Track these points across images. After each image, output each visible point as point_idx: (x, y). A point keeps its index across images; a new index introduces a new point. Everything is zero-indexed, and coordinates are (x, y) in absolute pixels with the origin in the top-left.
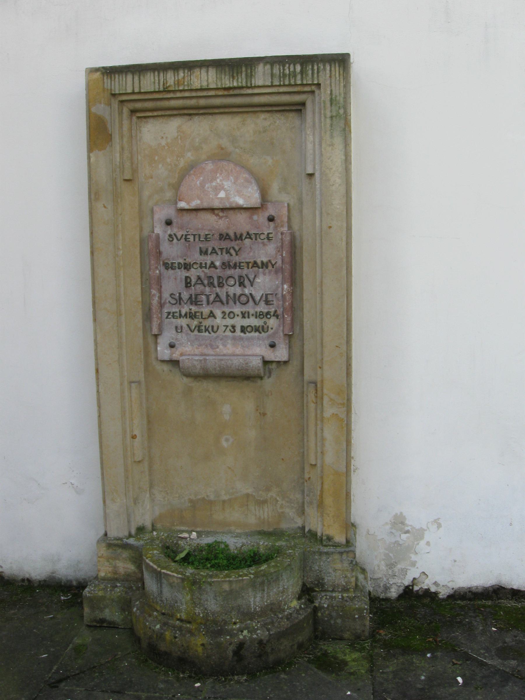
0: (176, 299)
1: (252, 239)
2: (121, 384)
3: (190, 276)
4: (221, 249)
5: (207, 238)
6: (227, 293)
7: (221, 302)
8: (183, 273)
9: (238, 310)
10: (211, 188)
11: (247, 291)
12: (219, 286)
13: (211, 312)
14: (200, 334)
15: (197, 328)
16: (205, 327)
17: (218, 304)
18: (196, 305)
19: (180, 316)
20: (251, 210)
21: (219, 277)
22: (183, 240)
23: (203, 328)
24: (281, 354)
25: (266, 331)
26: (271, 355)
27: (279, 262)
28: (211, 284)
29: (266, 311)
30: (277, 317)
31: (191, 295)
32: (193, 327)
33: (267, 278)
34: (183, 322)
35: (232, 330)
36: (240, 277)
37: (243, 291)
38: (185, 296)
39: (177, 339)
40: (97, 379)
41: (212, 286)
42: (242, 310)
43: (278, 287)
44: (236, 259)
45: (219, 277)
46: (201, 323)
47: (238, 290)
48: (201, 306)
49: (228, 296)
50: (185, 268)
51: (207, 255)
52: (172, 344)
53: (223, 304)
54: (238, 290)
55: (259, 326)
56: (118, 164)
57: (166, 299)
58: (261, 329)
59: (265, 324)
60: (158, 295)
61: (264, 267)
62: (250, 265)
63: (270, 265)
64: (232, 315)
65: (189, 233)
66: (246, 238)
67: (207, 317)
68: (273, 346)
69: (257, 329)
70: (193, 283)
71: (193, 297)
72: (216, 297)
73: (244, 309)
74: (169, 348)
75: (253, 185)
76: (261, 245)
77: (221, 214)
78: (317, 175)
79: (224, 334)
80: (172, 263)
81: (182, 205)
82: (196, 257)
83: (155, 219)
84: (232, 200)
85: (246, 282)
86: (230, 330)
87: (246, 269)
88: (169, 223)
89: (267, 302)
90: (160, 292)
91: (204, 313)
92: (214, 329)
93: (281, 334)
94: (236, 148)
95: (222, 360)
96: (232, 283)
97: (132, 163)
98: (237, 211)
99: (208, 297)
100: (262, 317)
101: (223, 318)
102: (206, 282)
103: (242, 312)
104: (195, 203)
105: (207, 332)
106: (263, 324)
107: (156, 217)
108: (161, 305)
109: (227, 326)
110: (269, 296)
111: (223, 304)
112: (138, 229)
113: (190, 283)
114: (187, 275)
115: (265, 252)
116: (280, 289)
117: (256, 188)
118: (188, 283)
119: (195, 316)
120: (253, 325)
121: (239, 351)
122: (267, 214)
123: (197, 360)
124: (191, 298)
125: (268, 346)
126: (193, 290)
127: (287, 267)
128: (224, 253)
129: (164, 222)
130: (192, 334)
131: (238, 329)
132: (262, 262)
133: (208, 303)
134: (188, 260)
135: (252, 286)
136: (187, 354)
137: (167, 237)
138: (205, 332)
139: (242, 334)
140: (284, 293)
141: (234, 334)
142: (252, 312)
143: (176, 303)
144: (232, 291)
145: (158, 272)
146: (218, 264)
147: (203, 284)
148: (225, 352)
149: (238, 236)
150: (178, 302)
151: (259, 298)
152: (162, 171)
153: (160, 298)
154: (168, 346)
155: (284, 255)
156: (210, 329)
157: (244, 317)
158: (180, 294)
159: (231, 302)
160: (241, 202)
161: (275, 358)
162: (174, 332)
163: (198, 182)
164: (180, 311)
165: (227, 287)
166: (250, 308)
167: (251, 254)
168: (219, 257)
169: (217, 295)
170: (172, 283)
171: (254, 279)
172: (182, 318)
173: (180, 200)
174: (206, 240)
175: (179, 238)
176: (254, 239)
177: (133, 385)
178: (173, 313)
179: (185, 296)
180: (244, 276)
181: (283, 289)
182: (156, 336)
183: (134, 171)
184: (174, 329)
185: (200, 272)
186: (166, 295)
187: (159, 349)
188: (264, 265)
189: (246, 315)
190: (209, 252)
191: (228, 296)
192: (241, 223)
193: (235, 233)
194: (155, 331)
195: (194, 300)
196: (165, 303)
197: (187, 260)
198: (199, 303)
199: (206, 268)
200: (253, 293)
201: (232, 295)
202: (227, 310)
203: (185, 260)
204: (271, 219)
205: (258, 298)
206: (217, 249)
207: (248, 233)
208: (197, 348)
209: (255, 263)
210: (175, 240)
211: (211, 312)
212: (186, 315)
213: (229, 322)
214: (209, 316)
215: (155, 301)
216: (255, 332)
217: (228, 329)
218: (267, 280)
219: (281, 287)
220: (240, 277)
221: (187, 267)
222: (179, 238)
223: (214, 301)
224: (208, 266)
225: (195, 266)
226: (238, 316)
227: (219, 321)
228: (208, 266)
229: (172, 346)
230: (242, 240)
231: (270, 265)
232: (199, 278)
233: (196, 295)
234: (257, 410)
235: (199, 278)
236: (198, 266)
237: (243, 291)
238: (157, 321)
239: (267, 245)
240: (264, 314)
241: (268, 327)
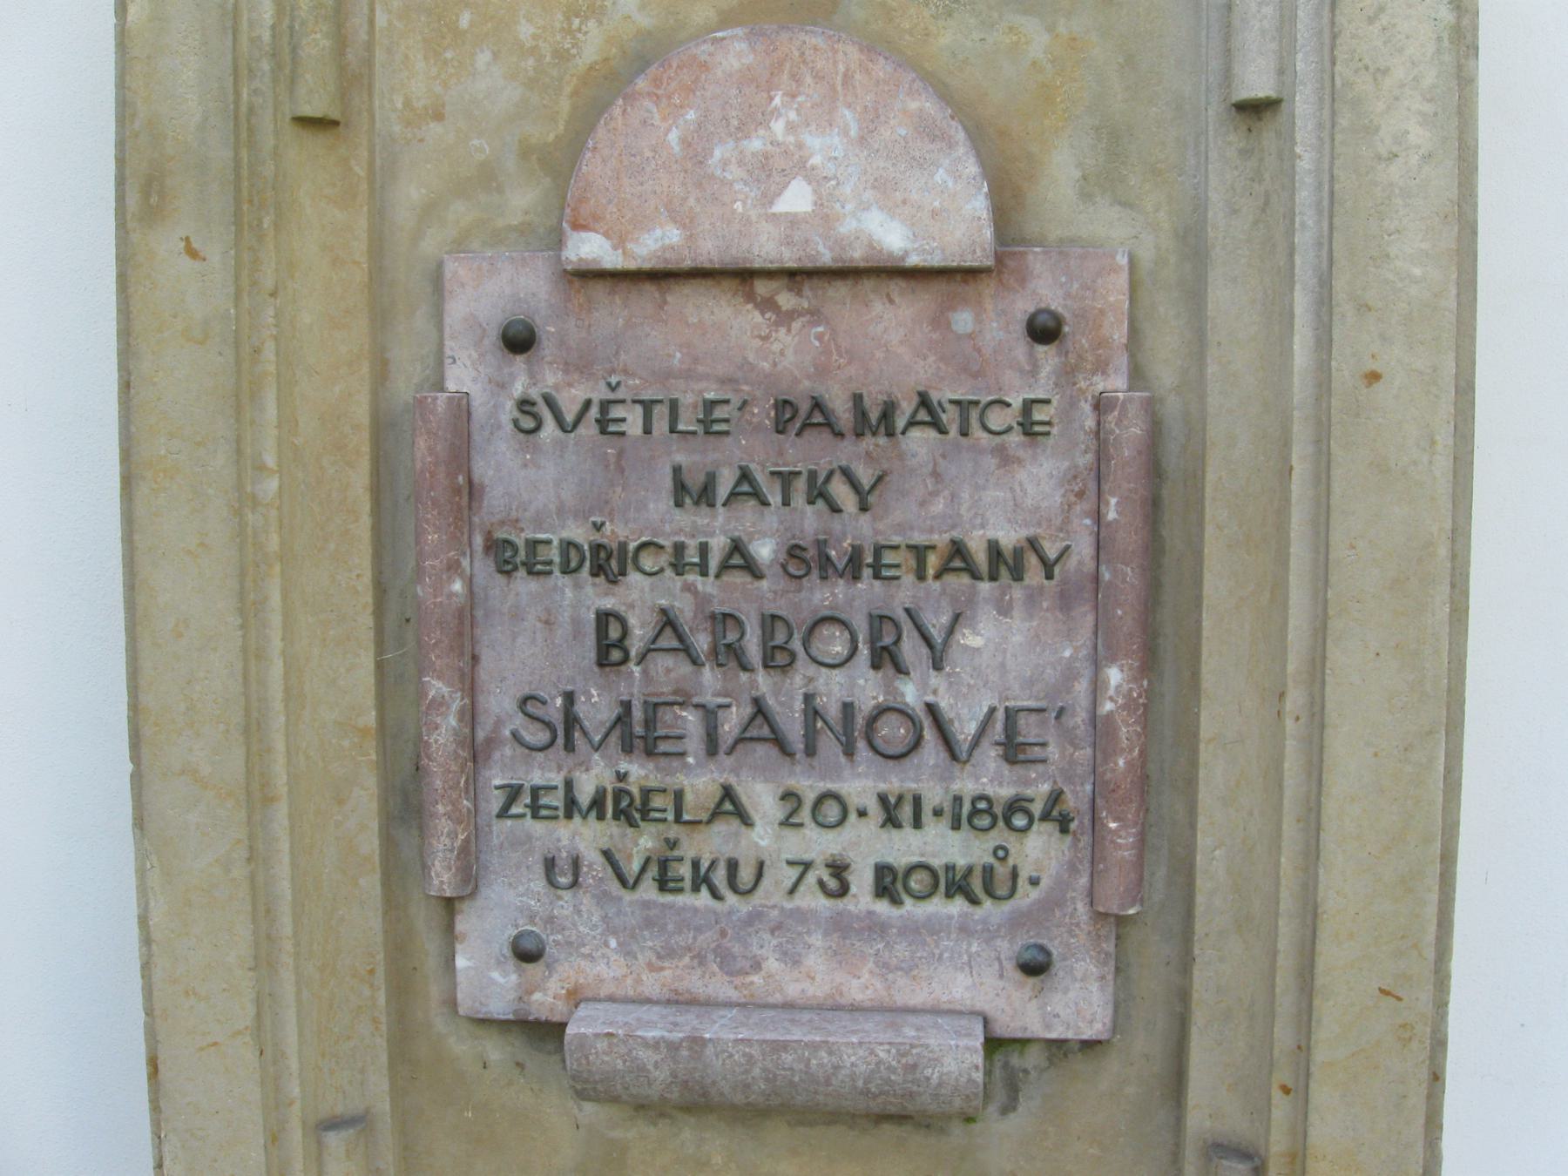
0: (548, 725)
1: (942, 431)
2: (274, 1138)
3: (622, 609)
4: (786, 480)
5: (710, 422)
6: (808, 698)
7: (779, 742)
8: (587, 597)
9: (861, 783)
10: (740, 163)
11: (910, 693)
12: (766, 666)
13: (728, 793)
15: (653, 871)
16: (696, 865)
18: (650, 753)
19: (571, 806)
21: (770, 621)
22: (588, 429)
23: (685, 870)
24: (1078, 1003)
25: (1002, 891)
27: (1083, 549)
28: (730, 655)
30: (1064, 824)
31: (627, 706)
32: (636, 866)
33: (1018, 629)
34: (585, 838)
35: (833, 884)
36: (879, 621)
38: (597, 708)
39: (550, 920)
40: (155, 1108)
41: (733, 664)
43: (1070, 676)
44: (855, 529)
45: (770, 621)
46: (673, 844)
47: (865, 687)
48: (676, 763)
49: (812, 712)
51: (712, 505)
52: (529, 945)
54: (865, 687)
55: (970, 870)
56: (266, 36)
57: (499, 723)
58: (977, 885)
59: (1003, 859)
61: (1004, 572)
62: (933, 561)
63: (1032, 560)
64: (832, 812)
65: (620, 394)
66: (912, 423)
67: (704, 816)
68: (1035, 967)
69: (957, 884)
70: (635, 649)
71: (638, 714)
72: (752, 719)
73: (896, 782)
74: (512, 963)
75: (961, 150)
76: (991, 462)
77: (786, 300)
78: (1304, 107)
79: (789, 905)
80: (533, 545)
81: (590, 248)
82: (653, 514)
83: (448, 321)
84: (847, 227)
85: (911, 648)
86: (821, 883)
87: (909, 579)
88: (519, 341)
89: (1014, 751)
90: (470, 687)
91: (689, 797)
92: (737, 878)
93: (1082, 908)
95: (784, 1046)
96: (839, 648)
97: (341, 42)
98: (868, 284)
99: (710, 716)
100: (985, 821)
101: (786, 823)
102: (702, 642)
103: (883, 799)
104: (655, 243)
105: (704, 891)
107: (457, 309)
108: (476, 753)
109: (807, 866)
110: (1022, 720)
112: (365, 369)
113: (620, 644)
114: (608, 603)
115: (1015, 497)
116: (1082, 687)
117: (972, 168)
118: (609, 644)
119: (645, 812)
120: (936, 863)
121: (861, 986)
122: (1023, 307)
123: (656, 1045)
125: (1009, 966)
126: (634, 682)
127: (1126, 576)
128: (799, 500)
129: (493, 335)
130: (628, 896)
131: (862, 880)
132: (994, 550)
133: (712, 746)
134: (617, 531)
135: (937, 666)
136: (603, 993)
137: (508, 411)
138: (696, 889)
139: (882, 907)
140: (1108, 706)
141: (840, 904)
142: (934, 795)
144: (833, 688)
145: (457, 586)
146: (764, 551)
147: (686, 650)
148: (793, 990)
149: (874, 416)
150: (560, 741)
151: (972, 728)
152: (490, 83)
153: (471, 715)
154: (507, 951)
155: (1112, 515)
156: (720, 877)
157: (892, 821)
158: (569, 698)
159: (829, 746)
160: (892, 237)
161: (1048, 1027)
162: (539, 884)
163: (673, 137)
164: (569, 785)
165: (812, 670)
166: (926, 777)
167: (939, 506)
169: (760, 710)
170: (532, 643)
171: (951, 631)
172: (577, 819)
173: (577, 227)
174: (707, 433)
175: (569, 418)
176: (954, 431)
177: (334, 1140)
178: (536, 792)
179: (597, 708)
181: (1097, 687)
182: (450, 905)
183: (353, 78)
184: (539, 869)
185: (674, 594)
186: (499, 703)
187: (461, 962)
188: (1004, 563)
189: (906, 812)
190: (723, 491)
191: (812, 712)
192: (890, 344)
193: (857, 399)
194: (443, 879)
195: (639, 732)
196: (492, 742)
197: (608, 527)
198: (663, 747)
199: (704, 574)
200: (944, 703)
201: (833, 712)
202: (809, 786)
203: (598, 527)
204: (1044, 331)
205: (965, 729)
206: (761, 478)
207: (924, 401)
208: (651, 967)
209: (958, 549)
210: (550, 429)
211: (728, 793)
212: (598, 803)
213: (818, 844)
214: (716, 814)
215: (444, 732)
217: (811, 878)
218: (1018, 638)
219: (1087, 673)
220: (879, 621)
221: (607, 563)
222: (569, 418)
223: (740, 740)
224: (713, 564)
225: (648, 562)
226: (862, 814)
227: (763, 837)
228: (713, 564)
229: (526, 954)
230: (890, 434)
231: (1032, 560)
232: (667, 621)
233: (653, 708)
235: (667, 621)
236: (664, 559)
237: (889, 689)
238: (453, 835)
239: (1019, 461)
240: (998, 810)
241: (1014, 875)
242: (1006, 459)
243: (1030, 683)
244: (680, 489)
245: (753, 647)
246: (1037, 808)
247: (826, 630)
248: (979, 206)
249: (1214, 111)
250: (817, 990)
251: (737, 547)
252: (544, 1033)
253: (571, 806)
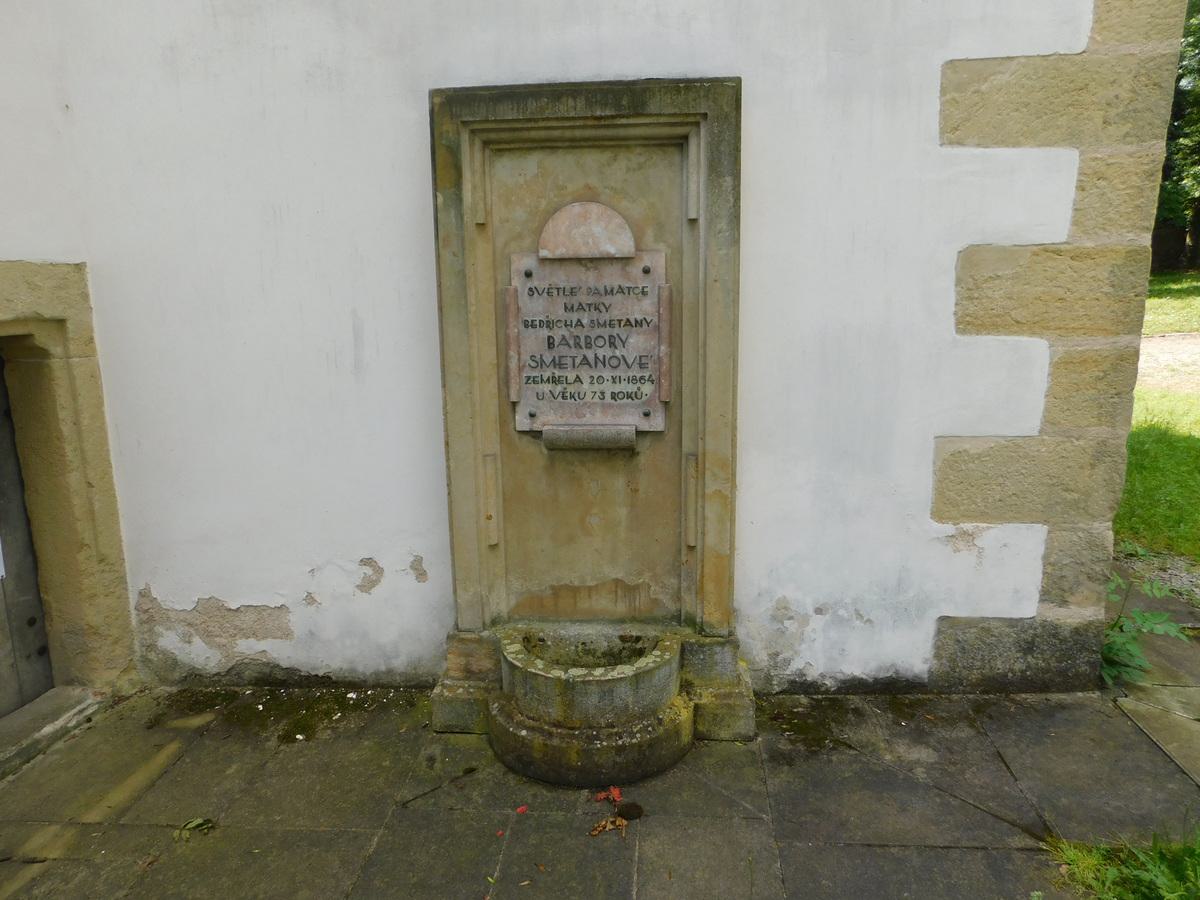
1: (624, 294)
4: (589, 305)
5: (573, 292)
7: (589, 364)
8: (545, 332)
9: (607, 374)
11: (618, 353)
12: (586, 347)
13: (578, 377)
19: (542, 380)
20: (625, 260)
21: (587, 337)
22: (545, 294)
23: (568, 395)
24: (657, 423)
25: (639, 397)
26: (645, 426)
27: (656, 320)
28: (578, 345)
29: (638, 376)
33: (641, 338)
34: (546, 388)
36: (611, 336)
38: (548, 359)
39: (537, 407)
40: (447, 452)
43: (654, 348)
44: (605, 317)
45: (587, 337)
46: (565, 389)
49: (596, 357)
50: (548, 326)
53: (590, 366)
54: (604, 352)
58: (633, 395)
60: (517, 357)
63: (644, 322)
68: (647, 415)
69: (629, 396)
70: (556, 344)
71: (557, 359)
73: (617, 373)
76: (635, 300)
77: (589, 265)
78: (702, 221)
80: (532, 321)
81: (544, 253)
87: (617, 326)
88: (528, 275)
89: (642, 366)
90: (519, 354)
92: (580, 396)
93: (657, 401)
94: (606, 188)
95: (591, 431)
96: (602, 344)
97: (485, 204)
99: (574, 358)
102: (571, 342)
104: (560, 252)
107: (513, 268)
108: (520, 369)
110: (643, 359)
111: (590, 366)
114: (550, 334)
117: (630, 235)
118: (551, 344)
121: (608, 420)
124: (554, 360)
125: (642, 415)
127: (665, 327)
128: (592, 310)
129: (523, 273)
131: (608, 396)
132: (636, 321)
133: (574, 366)
137: (527, 290)
139: (613, 401)
144: (601, 353)
145: (516, 330)
147: (568, 344)
149: (609, 290)
152: (520, 213)
153: (519, 359)
157: (614, 382)
159: (600, 365)
166: (621, 372)
167: (624, 310)
168: (586, 315)
169: (585, 357)
170: (533, 342)
177: (488, 458)
178: (534, 377)
179: (548, 359)
182: (514, 404)
183: (488, 213)
185: (564, 331)
186: (526, 357)
188: (638, 323)
190: (575, 308)
191: (596, 357)
194: (514, 398)
195: (558, 364)
196: (524, 366)
201: (601, 358)
203: (547, 317)
204: (646, 271)
207: (620, 287)
209: (628, 320)
210: (536, 294)
211: (578, 377)
213: (597, 387)
214: (575, 381)
217: (597, 396)
220: (611, 336)
221: (549, 324)
227: (586, 386)
229: (532, 415)
231: (644, 322)
232: (564, 337)
233: (560, 357)
235: (564, 337)
236: (563, 325)
242: (639, 300)
243: (644, 349)
244: (566, 308)
245: (583, 344)
246: (647, 378)
247: (600, 339)
248: (632, 243)
249: (685, 220)
250: (597, 421)
251: (579, 320)
253: (542, 380)
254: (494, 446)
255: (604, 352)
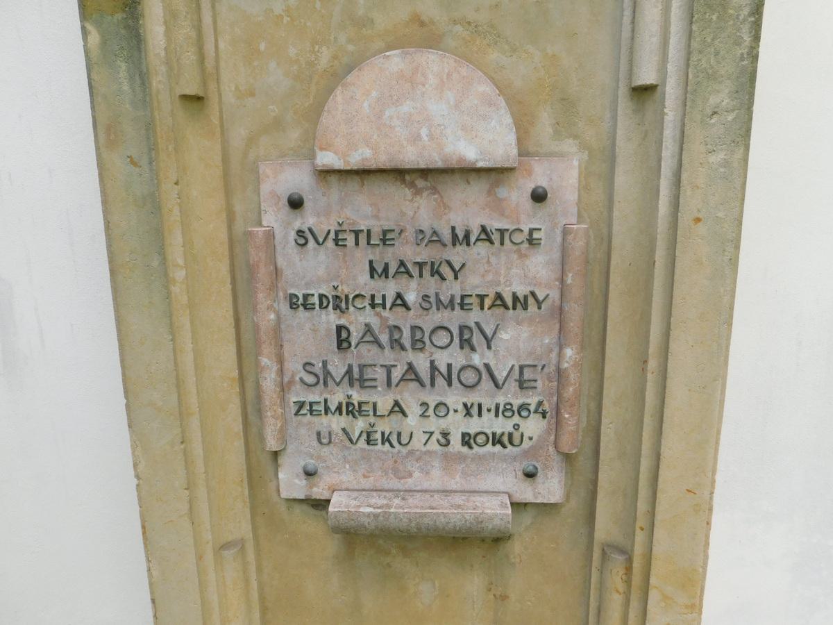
0: (316, 375)
1: (492, 243)
2: (200, 558)
3: (347, 325)
4: (421, 265)
5: (386, 239)
6: (432, 362)
7: (418, 380)
8: (331, 318)
9: (454, 399)
10: (398, 118)
11: (477, 360)
12: (413, 349)
13: (397, 404)
14: (372, 447)
15: (364, 436)
16: (383, 434)
17: (414, 385)
18: (362, 387)
19: (327, 410)
20: (495, 174)
21: (414, 328)
22: (330, 243)
23: (378, 436)
24: (551, 488)
26: (526, 493)
27: (555, 295)
28: (397, 344)
29: (516, 403)
30: (544, 415)
31: (350, 367)
32: (357, 435)
33: (525, 332)
34: (336, 423)
35: (443, 441)
36: (462, 328)
37: (468, 358)
39: (319, 458)
41: (398, 348)
42: (465, 400)
44: (452, 289)
45: (414, 328)
46: (373, 426)
48: (373, 391)
49: (433, 367)
50: (336, 307)
51: (387, 277)
52: (310, 468)
53: (422, 385)
55: (503, 434)
56: (163, 53)
57: (293, 376)
59: (518, 429)
60: (275, 368)
61: (519, 305)
62: (487, 302)
63: (531, 300)
64: (442, 411)
65: (344, 227)
66: (478, 240)
67: (387, 413)
68: (530, 475)
69: (497, 440)
70: (354, 342)
71: (356, 370)
72: (407, 371)
73: (473, 398)
74: (303, 476)
75: (503, 111)
77: (420, 183)
78: (672, 90)
79: (424, 449)
80: (306, 297)
81: (327, 159)
82: (362, 282)
83: (262, 194)
84: (449, 149)
85: (477, 339)
86: (438, 441)
87: (476, 308)
88: (296, 204)
89: (522, 384)
90: (281, 361)
91: (379, 405)
94: (455, 22)
96: (446, 341)
98: (457, 176)
99: (389, 369)
100: (508, 414)
101: (423, 415)
102: (384, 338)
103: (465, 405)
104: (357, 158)
105: (387, 444)
106: (511, 429)
107: (265, 188)
109: (432, 433)
110: (526, 370)
111: (422, 385)
112: (224, 215)
113: (347, 340)
114: (342, 322)
116: (554, 355)
117: (508, 120)
118: (342, 339)
119: (360, 411)
120: (489, 432)
121: (456, 482)
122: (530, 186)
123: (369, 515)
124: (349, 372)
125: (520, 474)
126: (352, 358)
129: (285, 201)
130: (353, 447)
131: (456, 439)
132: (515, 298)
133: (389, 383)
134: (344, 289)
135: (489, 347)
136: (344, 487)
137: (292, 235)
138: (383, 443)
139: (465, 449)
140: (566, 365)
141: (446, 449)
142: (487, 403)
143: (318, 383)
145: (272, 316)
146: (411, 298)
147: (377, 342)
148: (426, 485)
149: (461, 237)
150: (322, 382)
151: (505, 374)
153: (281, 372)
154: (301, 471)
155: (569, 281)
158: (325, 363)
159: (440, 381)
160: (470, 152)
161: (536, 498)
162: (315, 443)
163: (366, 104)
164: (326, 401)
165: (434, 350)
166: (484, 396)
168: (414, 284)
169: (411, 367)
170: (309, 336)
171: (495, 333)
172: (330, 415)
173: (321, 149)
174: (384, 244)
175: (321, 240)
176: (497, 243)
177: (228, 554)
178: (311, 404)
180: (473, 325)
181: (560, 355)
182: (276, 455)
184: (315, 436)
185: (369, 316)
186: (294, 366)
187: (281, 476)
189: (475, 411)
190: (392, 271)
191: (433, 367)
193: (453, 228)
194: (272, 444)
195: (357, 378)
196: (291, 382)
197: (340, 288)
198: (367, 384)
199: (384, 308)
200: (492, 364)
201: (444, 369)
202: (432, 400)
203: (335, 288)
204: (539, 197)
205: (500, 376)
206: (410, 266)
207: (484, 229)
208: (365, 476)
209: (499, 296)
210: (312, 243)
211: (397, 404)
212: (339, 409)
213: (434, 424)
214: (391, 412)
215: (269, 382)
216: (494, 444)
217: (434, 438)
218: (526, 335)
219: (556, 350)
221: (339, 303)
222: (321, 240)
223: (401, 380)
224: (388, 305)
225: (358, 303)
226: (456, 411)
227: (412, 421)
228: (388, 305)
229: (309, 474)
230: (468, 244)
231: (531, 300)
232: (368, 329)
233: (362, 367)
234: (490, 590)
235: (368, 329)
236: (366, 303)
237: (468, 358)
238: (275, 425)
239: (526, 256)
240: (515, 409)
241: (522, 435)
242: (522, 256)
243: (530, 354)
244: (372, 270)
245: (406, 340)
246: (532, 408)
247: (442, 333)
248: (512, 138)
249: (623, 91)
250: (435, 485)
251: (399, 296)
252: (321, 505)
253: (327, 410)
254: (241, 527)
255: (452, 357)
